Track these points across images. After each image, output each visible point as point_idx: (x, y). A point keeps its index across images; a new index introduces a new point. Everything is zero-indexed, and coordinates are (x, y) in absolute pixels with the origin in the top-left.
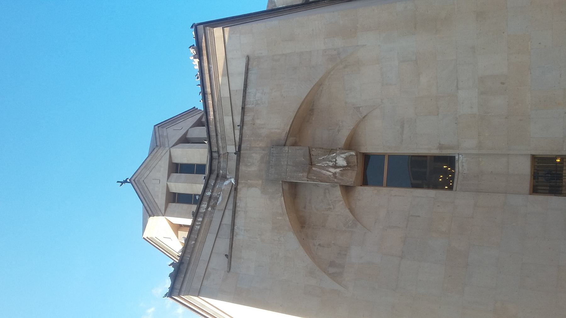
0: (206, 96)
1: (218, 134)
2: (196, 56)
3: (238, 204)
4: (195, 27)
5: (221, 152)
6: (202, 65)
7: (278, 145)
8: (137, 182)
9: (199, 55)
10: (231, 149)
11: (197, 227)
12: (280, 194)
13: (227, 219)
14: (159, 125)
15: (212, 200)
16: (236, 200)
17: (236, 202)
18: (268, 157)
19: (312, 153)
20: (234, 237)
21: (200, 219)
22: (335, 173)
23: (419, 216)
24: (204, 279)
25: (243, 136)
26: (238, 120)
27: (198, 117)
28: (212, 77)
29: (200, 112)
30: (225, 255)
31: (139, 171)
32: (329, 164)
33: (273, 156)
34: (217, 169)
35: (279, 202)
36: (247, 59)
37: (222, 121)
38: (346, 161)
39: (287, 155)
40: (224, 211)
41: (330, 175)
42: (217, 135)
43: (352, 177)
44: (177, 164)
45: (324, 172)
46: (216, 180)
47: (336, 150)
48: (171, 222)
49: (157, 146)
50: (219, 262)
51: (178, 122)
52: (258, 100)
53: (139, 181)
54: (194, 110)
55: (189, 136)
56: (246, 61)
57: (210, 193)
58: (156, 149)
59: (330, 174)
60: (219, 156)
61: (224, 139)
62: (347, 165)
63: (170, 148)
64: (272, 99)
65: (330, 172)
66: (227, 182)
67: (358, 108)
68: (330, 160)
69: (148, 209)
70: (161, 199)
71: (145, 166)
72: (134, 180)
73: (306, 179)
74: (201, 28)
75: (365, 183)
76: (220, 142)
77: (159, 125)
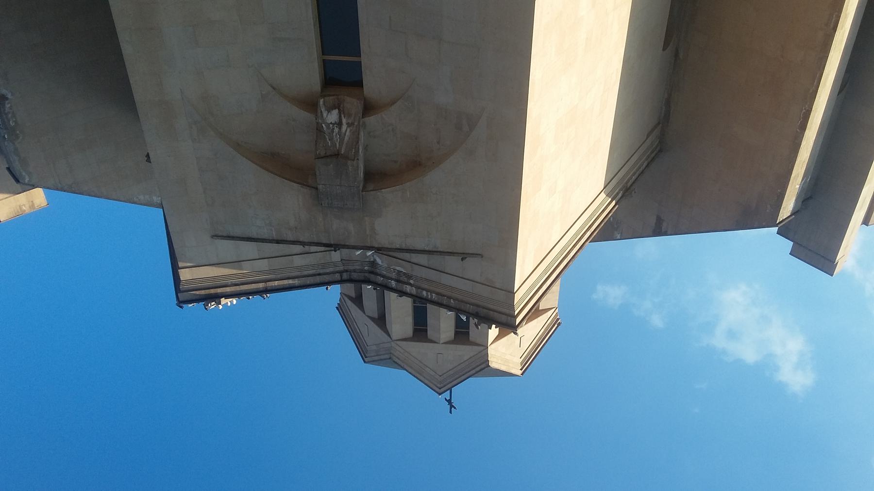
0: (269, 288)
1: (317, 273)
2: (217, 302)
3: (398, 246)
4: (181, 303)
5: (341, 268)
6: (229, 294)
9: (216, 298)
10: (336, 256)
11: (434, 297)
12: (379, 193)
13: (422, 259)
15: (401, 279)
16: (393, 249)
17: (396, 249)
18: (335, 210)
19: (323, 153)
20: (439, 250)
21: (424, 293)
22: (348, 124)
23: (390, 17)
24: (494, 286)
25: (313, 241)
26: (298, 248)
27: (349, 303)
28: (243, 282)
29: (342, 299)
30: (462, 260)
31: (426, 382)
32: (337, 132)
33: (332, 203)
34: (363, 274)
35: (388, 194)
36: (216, 237)
38: (332, 110)
39: (328, 186)
40: (412, 263)
41: (350, 131)
42: (319, 274)
43: (353, 104)
44: (415, 331)
45: (346, 138)
46: (377, 274)
47: (317, 123)
48: (497, 336)
49: (390, 358)
50: (472, 268)
51: (358, 331)
55: (376, 316)
56: (218, 239)
57: (392, 281)
58: (394, 359)
59: (348, 130)
60: (347, 271)
62: (337, 109)
63: (393, 341)
65: (346, 131)
66: (379, 261)
68: (332, 132)
70: (464, 352)
71: (419, 374)
72: (440, 389)
73: (355, 161)
74: (182, 296)
75: (359, 84)
76: (328, 271)
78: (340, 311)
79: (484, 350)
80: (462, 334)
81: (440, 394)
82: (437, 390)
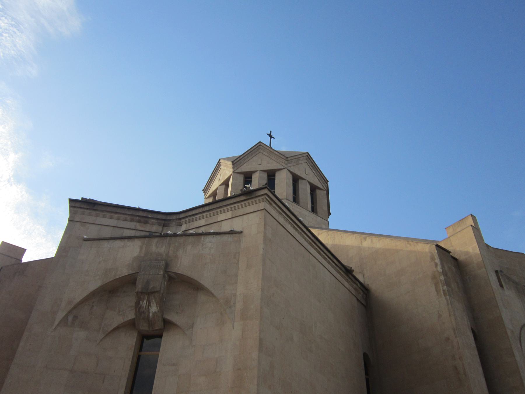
5: (182, 221)
7: (167, 265)
8: (259, 147)
13: (127, 233)
14: (309, 156)
19: (157, 294)
23: (103, 383)
27: (320, 186)
35: (125, 272)
37: (203, 218)
43: (144, 327)
44: (274, 176)
49: (287, 158)
50: (93, 231)
52: (206, 245)
53: (260, 148)
54: (326, 182)
61: (191, 221)
63: (286, 168)
64: (205, 257)
67: (192, 327)
69: (238, 159)
70: (246, 168)
72: (260, 145)
76: (189, 218)
77: (309, 156)
78: (326, 180)
79: (235, 171)
80: (248, 178)
81: (260, 142)
82: (261, 144)
